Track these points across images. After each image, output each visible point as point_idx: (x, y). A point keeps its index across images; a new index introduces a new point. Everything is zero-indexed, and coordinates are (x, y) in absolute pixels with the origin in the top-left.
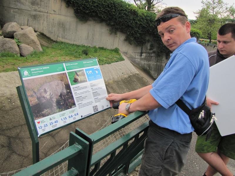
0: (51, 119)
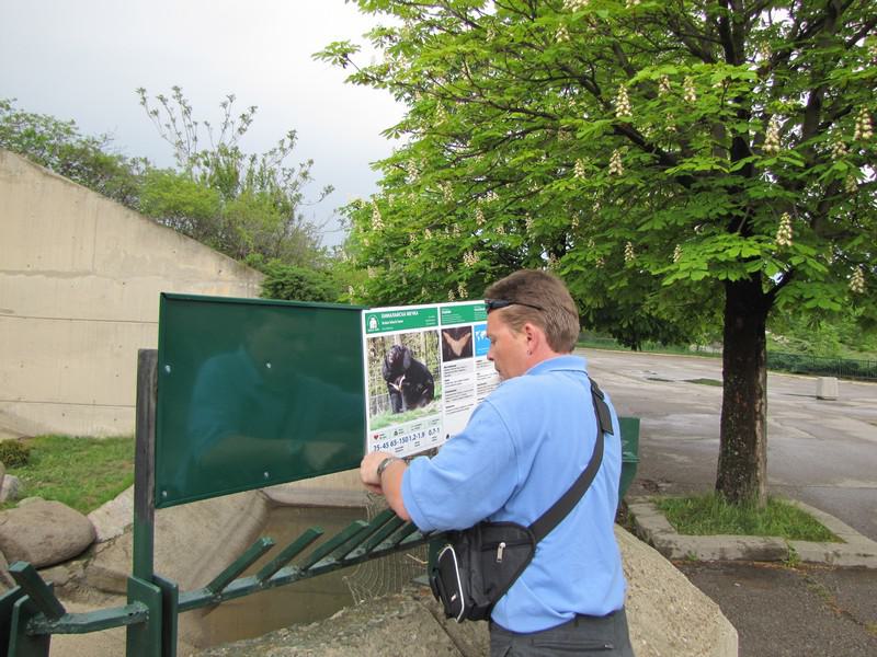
0: (396, 433)
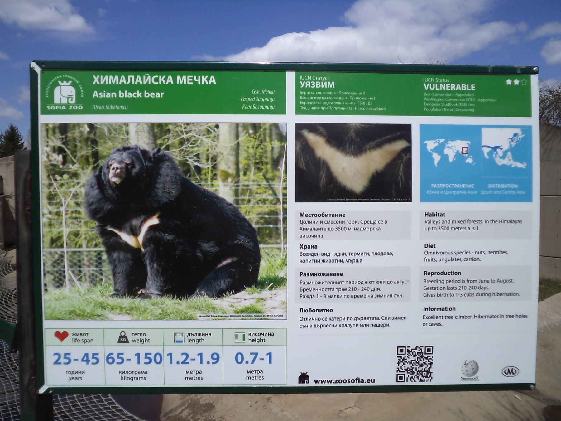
0: (123, 339)
